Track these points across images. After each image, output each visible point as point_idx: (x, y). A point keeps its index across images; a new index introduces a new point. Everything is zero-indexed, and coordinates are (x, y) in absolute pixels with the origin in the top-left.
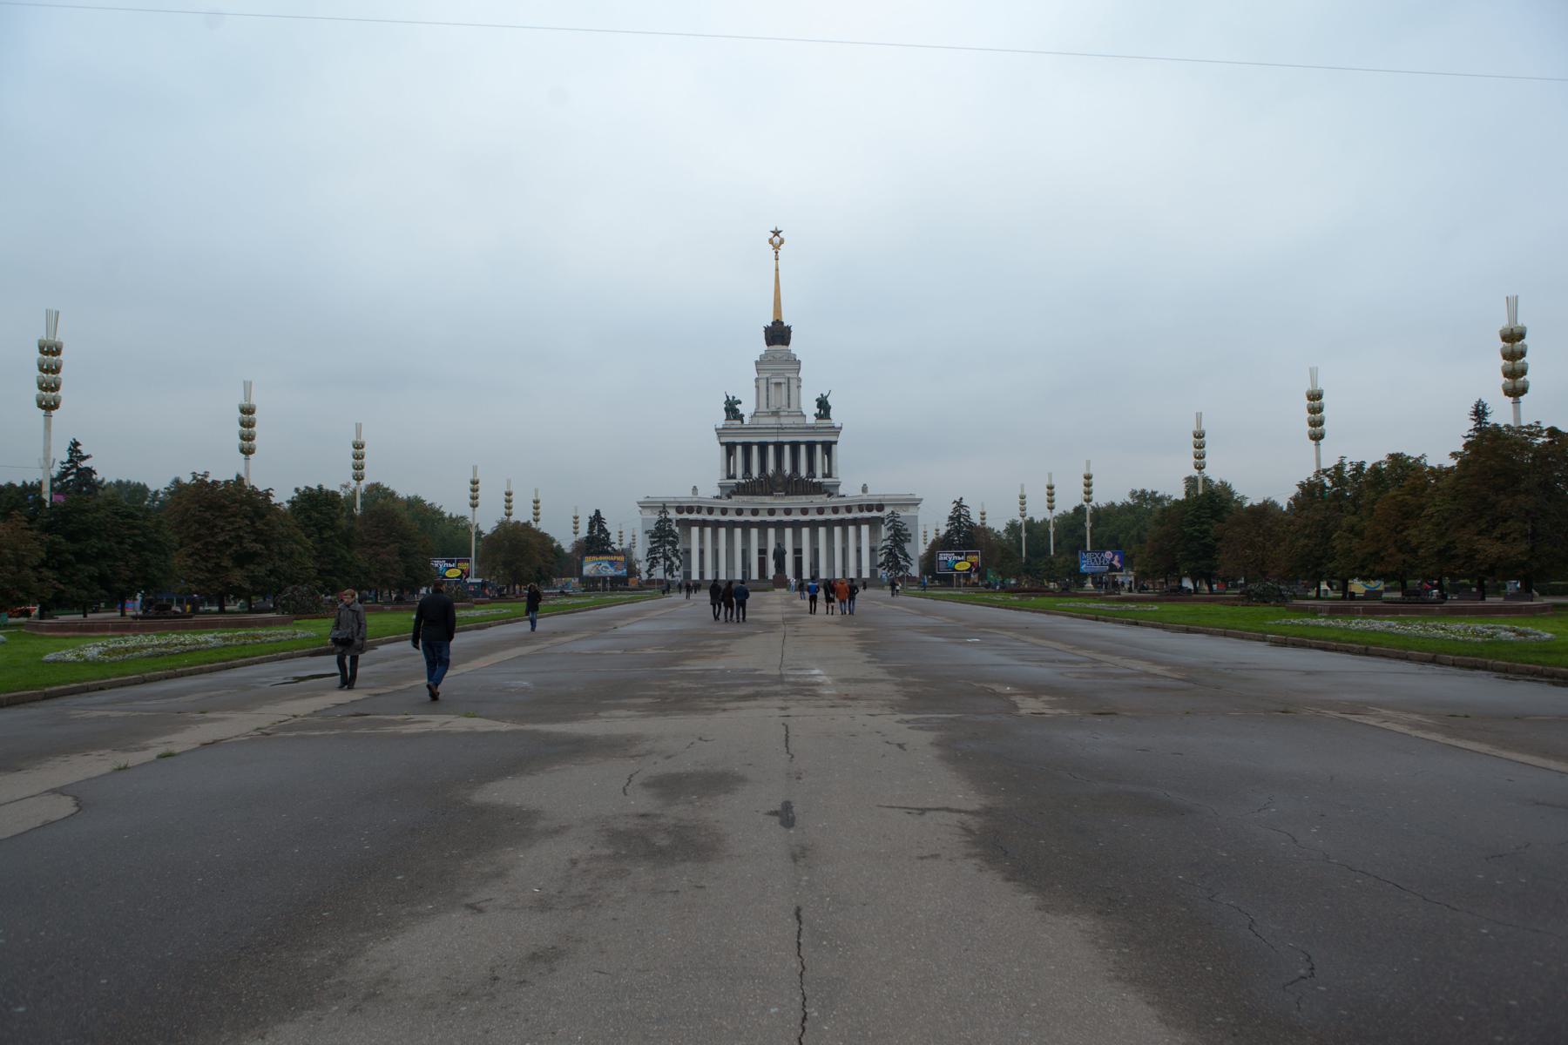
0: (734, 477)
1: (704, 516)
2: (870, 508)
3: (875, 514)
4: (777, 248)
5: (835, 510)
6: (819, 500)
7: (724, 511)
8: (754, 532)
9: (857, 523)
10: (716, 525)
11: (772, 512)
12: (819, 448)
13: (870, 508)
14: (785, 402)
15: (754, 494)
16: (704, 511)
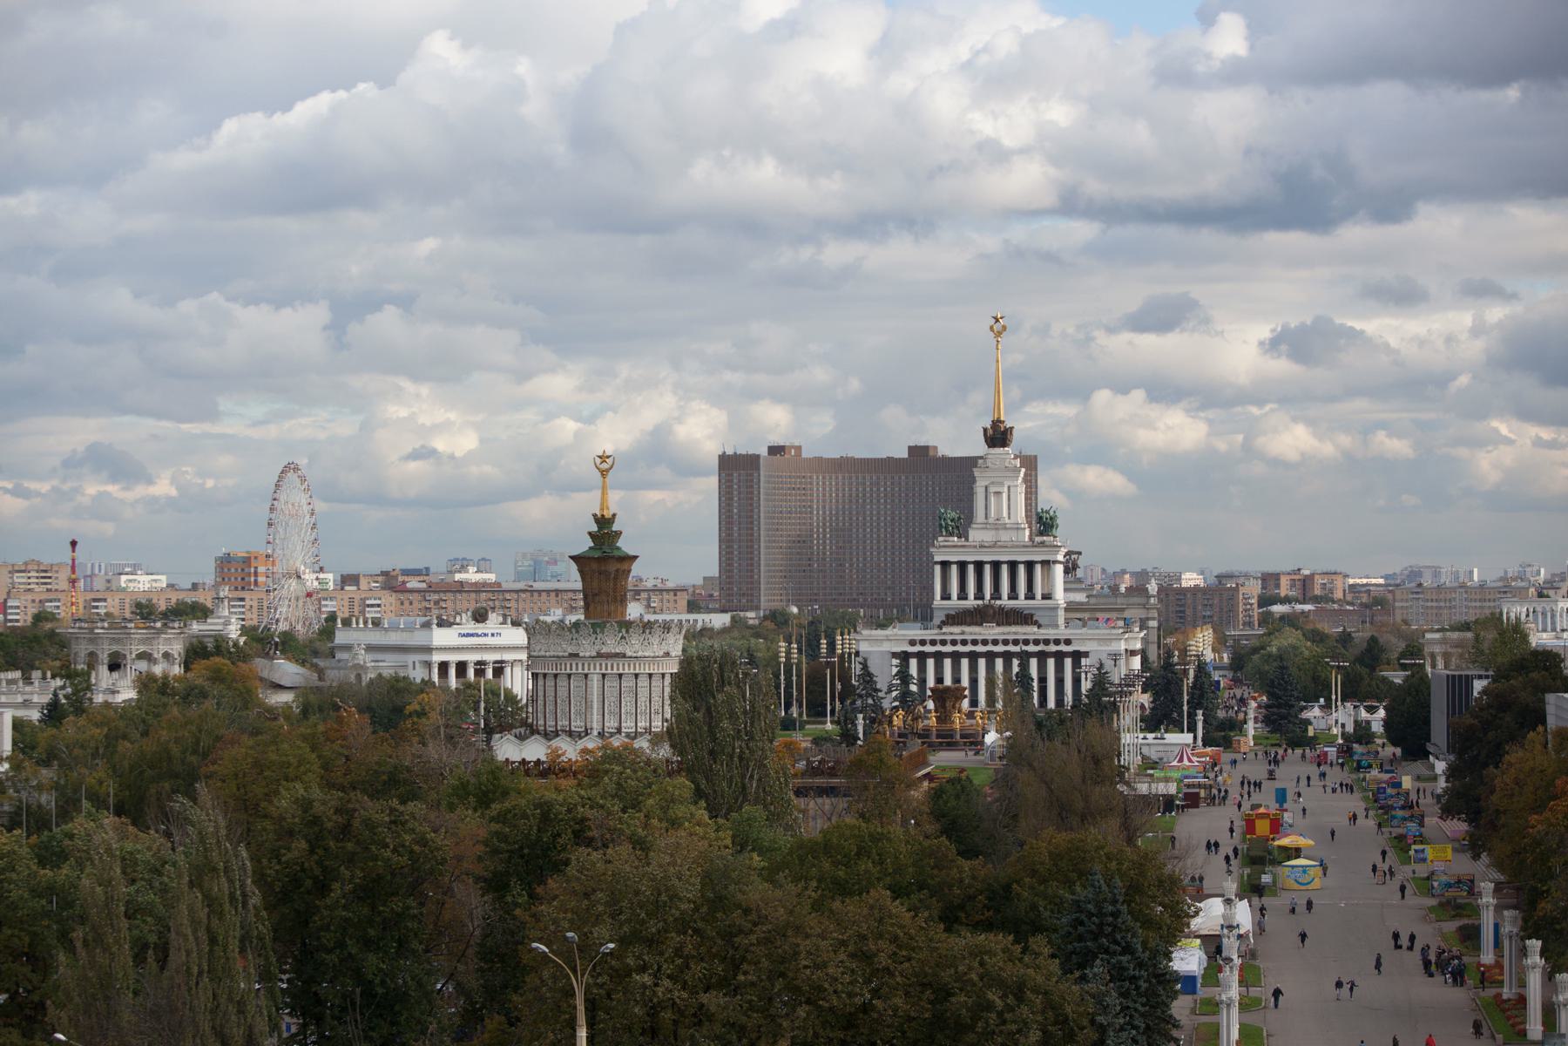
0: (949, 598)
6: (1030, 631)
12: (1038, 568)
14: (1005, 514)
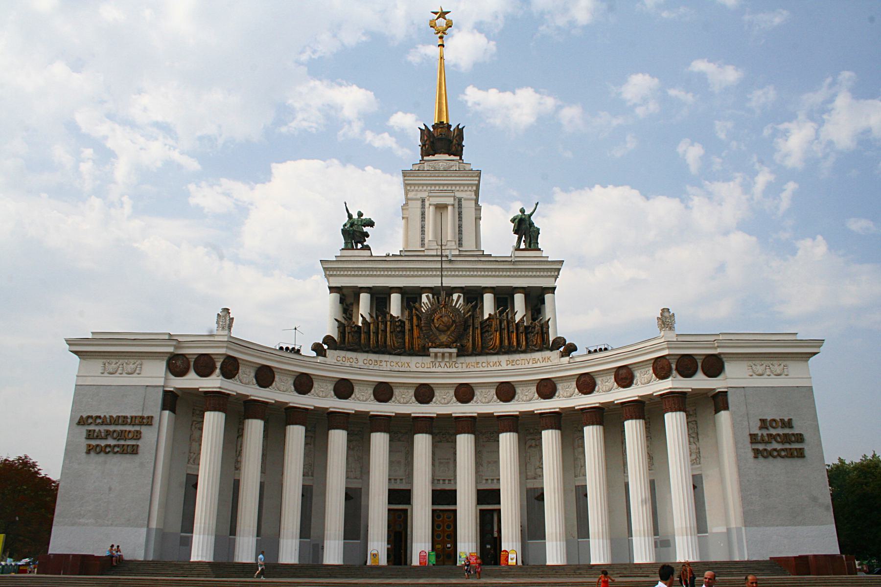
1: (243, 386)
2: (686, 365)
3: (700, 382)
5: (586, 384)
7: (303, 384)
8: (379, 441)
9: (649, 411)
10: (279, 418)
11: (424, 394)
13: (686, 365)
15: (382, 349)
16: (247, 374)
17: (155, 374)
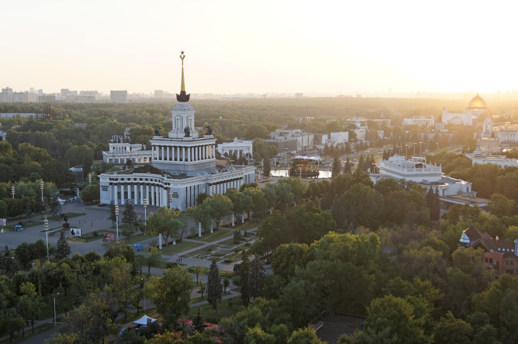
2: (166, 184)
3: (167, 186)
4: (183, 59)
13: (166, 184)
17: (108, 181)
